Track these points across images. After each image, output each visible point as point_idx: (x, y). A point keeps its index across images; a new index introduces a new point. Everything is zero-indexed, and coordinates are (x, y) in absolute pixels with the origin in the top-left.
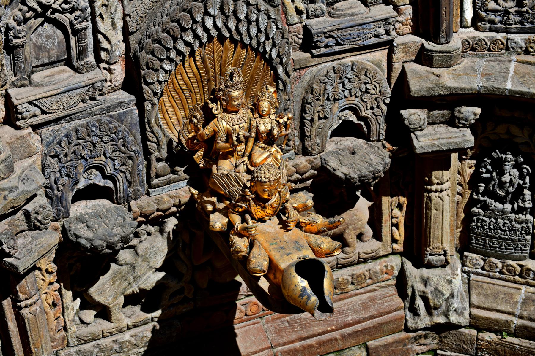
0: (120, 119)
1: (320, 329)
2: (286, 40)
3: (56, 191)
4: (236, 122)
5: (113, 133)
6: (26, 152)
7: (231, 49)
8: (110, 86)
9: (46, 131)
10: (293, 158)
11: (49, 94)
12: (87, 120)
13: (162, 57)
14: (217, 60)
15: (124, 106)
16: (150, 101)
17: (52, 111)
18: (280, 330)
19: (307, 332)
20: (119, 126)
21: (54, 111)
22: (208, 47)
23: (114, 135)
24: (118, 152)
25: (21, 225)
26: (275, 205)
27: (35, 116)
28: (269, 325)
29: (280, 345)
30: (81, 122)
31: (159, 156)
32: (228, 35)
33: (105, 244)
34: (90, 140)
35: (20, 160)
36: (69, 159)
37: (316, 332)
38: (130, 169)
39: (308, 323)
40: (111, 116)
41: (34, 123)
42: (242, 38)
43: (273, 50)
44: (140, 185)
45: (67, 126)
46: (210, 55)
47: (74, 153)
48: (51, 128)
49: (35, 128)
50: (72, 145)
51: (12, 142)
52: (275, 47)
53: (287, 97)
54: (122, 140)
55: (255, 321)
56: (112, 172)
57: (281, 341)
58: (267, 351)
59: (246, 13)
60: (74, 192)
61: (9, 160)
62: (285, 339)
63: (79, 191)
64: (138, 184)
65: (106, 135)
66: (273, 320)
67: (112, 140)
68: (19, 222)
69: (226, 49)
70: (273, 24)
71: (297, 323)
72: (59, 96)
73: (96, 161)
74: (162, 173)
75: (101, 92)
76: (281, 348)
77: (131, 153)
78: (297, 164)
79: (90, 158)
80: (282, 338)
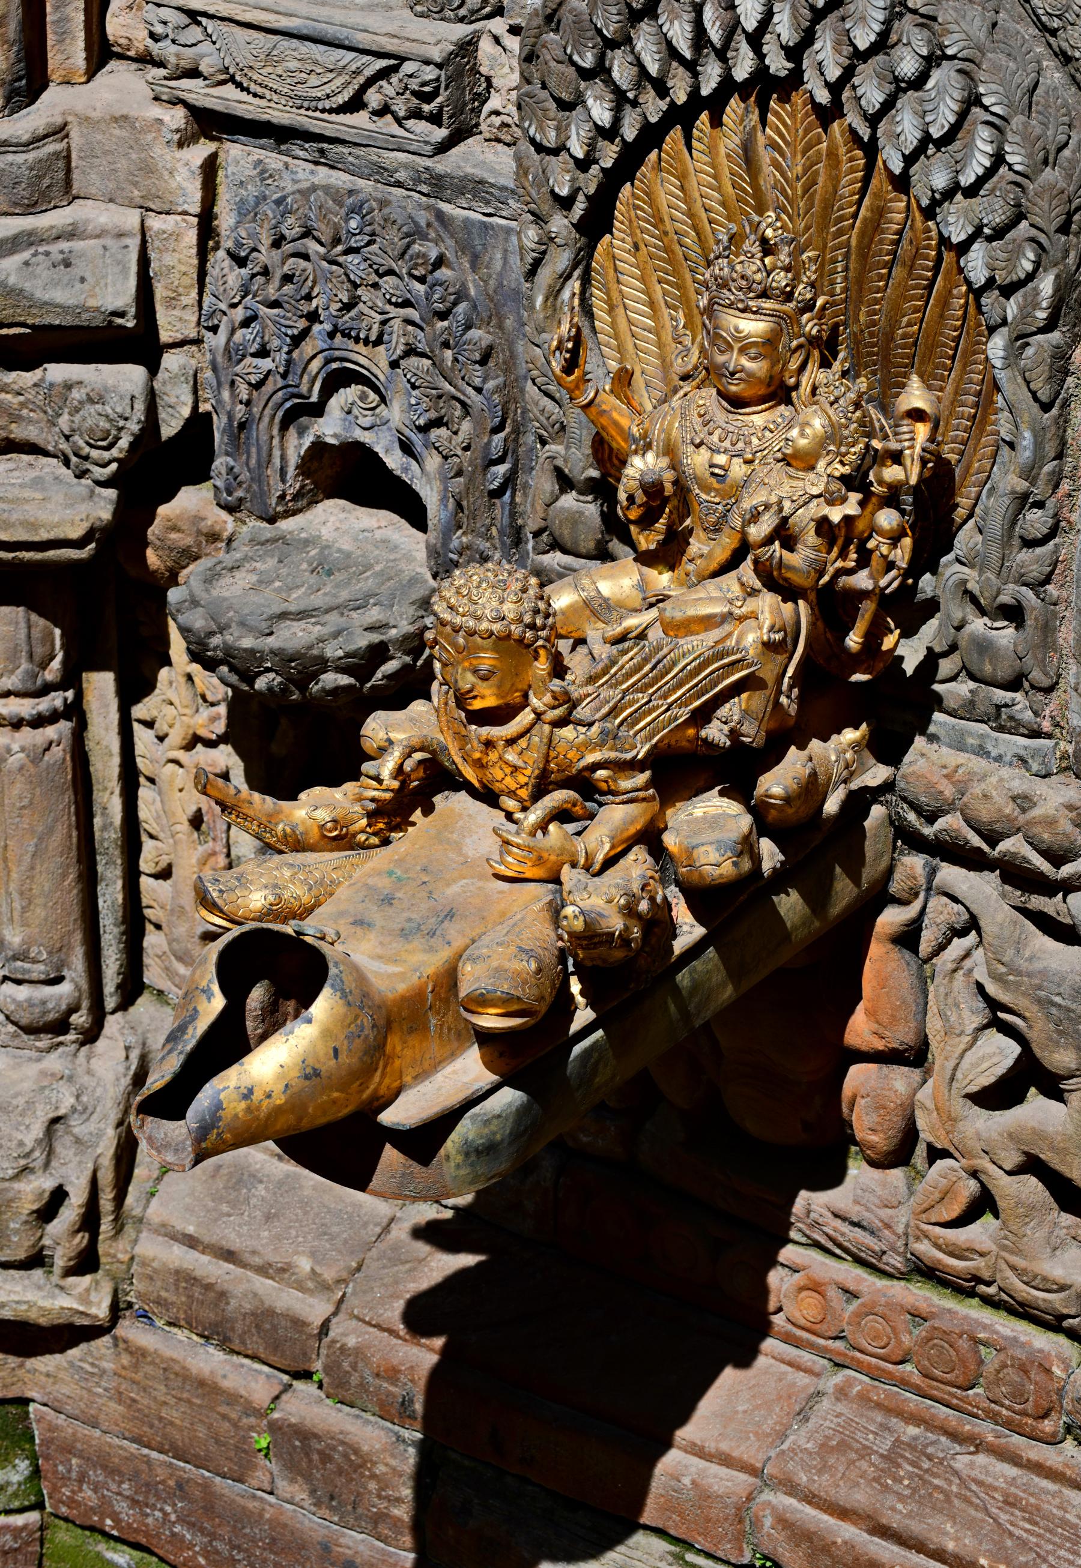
0: (472, 245)
1: (957, 1539)
2: (1034, 232)
3: (226, 395)
4: (715, 438)
5: (422, 280)
6: (135, 184)
7: (852, 170)
8: (497, 113)
9: (239, 157)
10: (1035, 767)
11: (249, 17)
12: (365, 185)
13: (576, 58)
14: (806, 191)
15: (487, 203)
16: (539, 219)
17: (253, 87)
18: (843, 1446)
19: (910, 1515)
20: (440, 262)
21: (259, 90)
22: (777, 114)
23: (420, 288)
24: (427, 362)
25: (30, 421)
26: (511, 756)
27: (193, 73)
28: (840, 1408)
29: (791, 1488)
30: (340, 179)
31: (559, 462)
32: (823, 96)
33: (216, 641)
34: (341, 259)
35: (111, 201)
36: (272, 291)
37: (935, 1540)
38: (459, 453)
39: (947, 1495)
40: (440, 215)
41: (190, 98)
42: (874, 138)
43: (976, 246)
44: (503, 543)
45: (298, 171)
46: (782, 155)
47: (287, 279)
48: (258, 154)
49: (209, 123)
50: (288, 248)
51: (87, 119)
52: (990, 239)
53: (1022, 485)
54: (446, 323)
55: (806, 1357)
56: (407, 432)
57: (803, 1478)
58: (743, 1477)
59: (877, 27)
60: (308, 441)
61: (10, 157)
62: (822, 1484)
63: (319, 447)
64: (494, 531)
65: (391, 272)
66: (863, 1398)
67: (406, 304)
68: (23, 405)
69: (832, 154)
70: (985, 132)
71: (914, 1464)
72: (285, 43)
73: (361, 357)
74: (566, 535)
75: (426, 108)
76: (792, 1501)
77: (470, 391)
78: (1026, 797)
79: (346, 335)
80: (820, 1472)
